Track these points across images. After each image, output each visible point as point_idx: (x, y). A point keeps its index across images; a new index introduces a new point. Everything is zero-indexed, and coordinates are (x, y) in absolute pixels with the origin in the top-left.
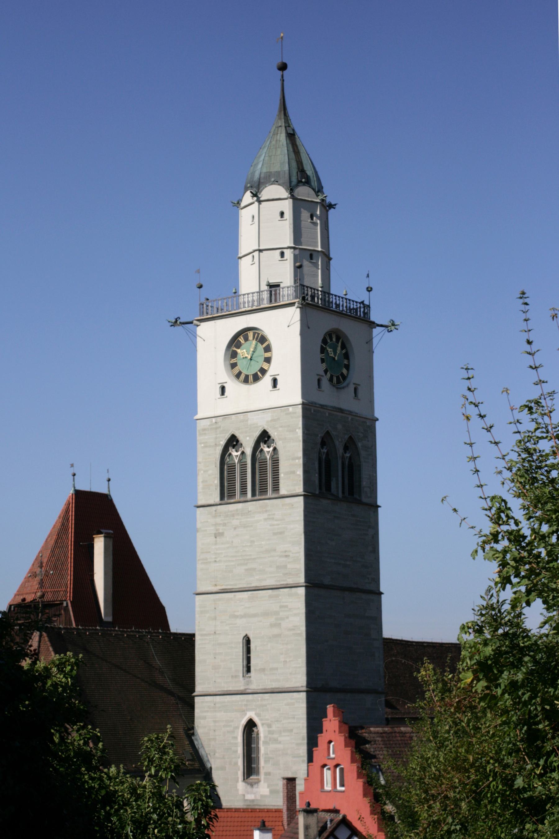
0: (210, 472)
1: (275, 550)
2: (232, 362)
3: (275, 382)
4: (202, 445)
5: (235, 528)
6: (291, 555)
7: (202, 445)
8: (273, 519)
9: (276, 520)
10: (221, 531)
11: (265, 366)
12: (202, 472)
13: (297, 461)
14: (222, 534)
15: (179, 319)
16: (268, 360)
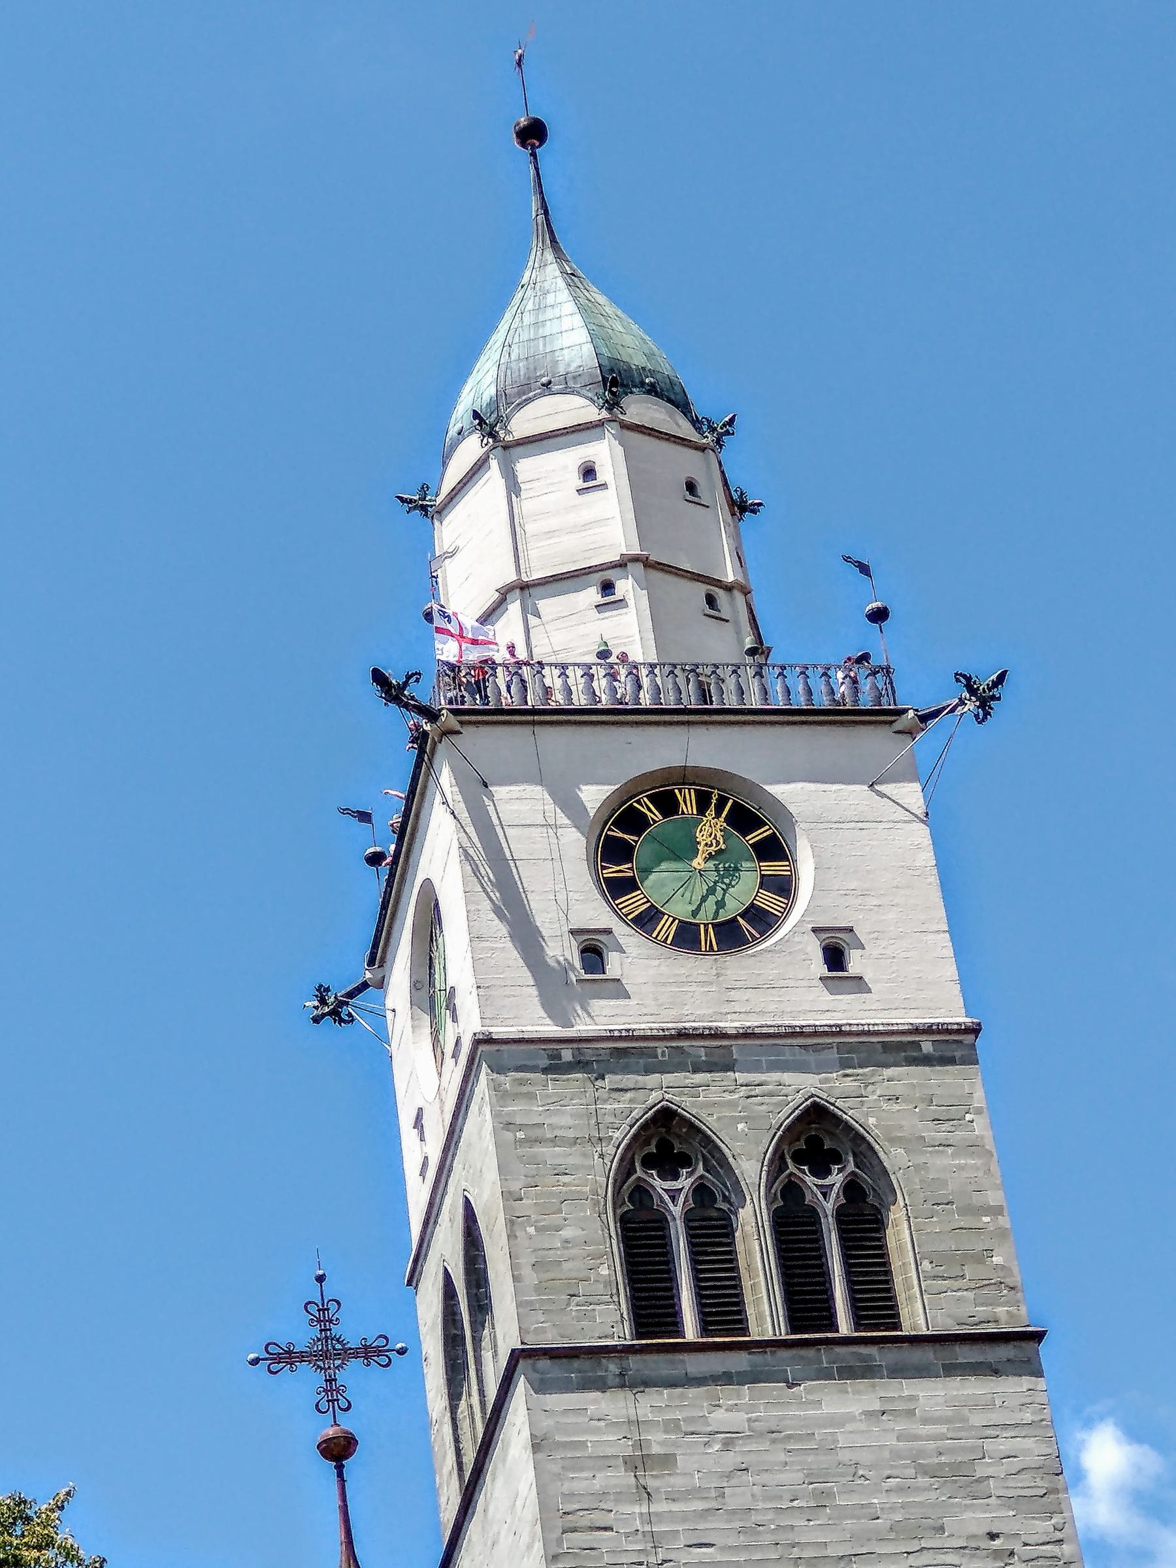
0: (567, 1233)
1: (941, 1529)
2: (612, 871)
3: (835, 957)
4: (520, 1135)
5: (727, 1445)
6: (1018, 1548)
7: (520, 1135)
8: (911, 1413)
9: (925, 1421)
10: (656, 1449)
11: (769, 901)
12: (531, 1230)
13: (986, 1219)
14: (667, 1461)
15: (417, 681)
16: (784, 887)
